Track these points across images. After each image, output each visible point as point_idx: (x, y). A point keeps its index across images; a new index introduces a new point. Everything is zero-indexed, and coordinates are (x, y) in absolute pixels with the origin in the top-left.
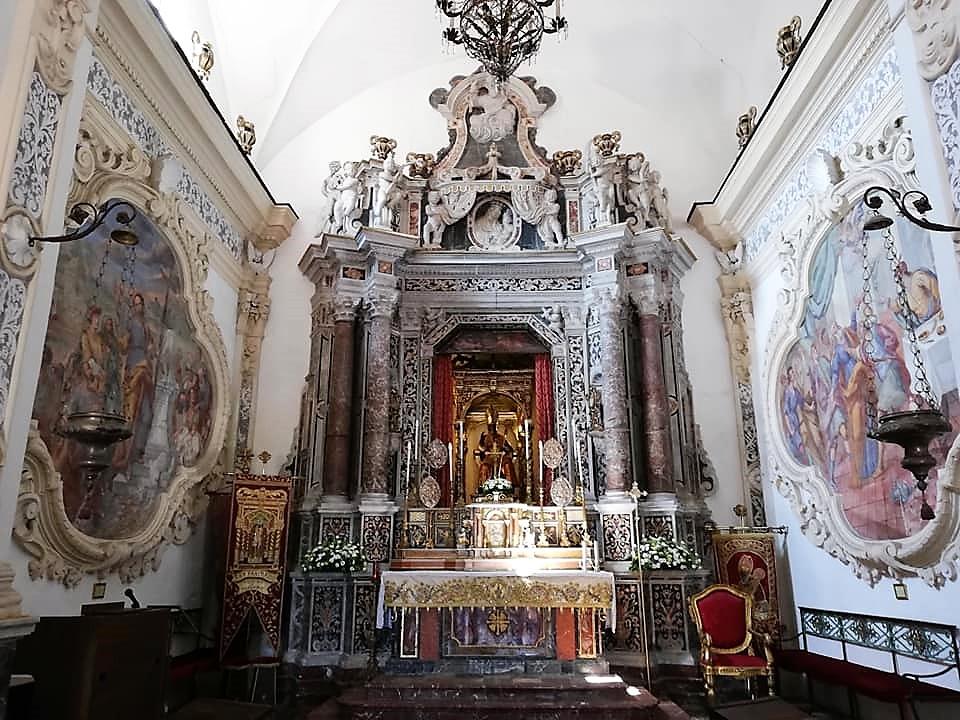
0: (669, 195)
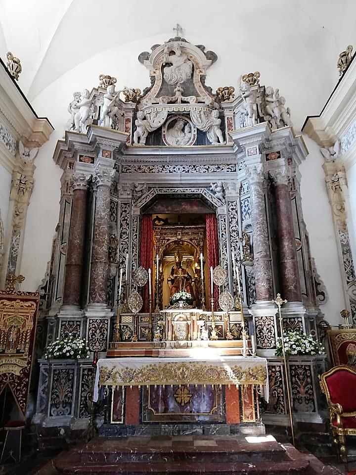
0: (291, 112)
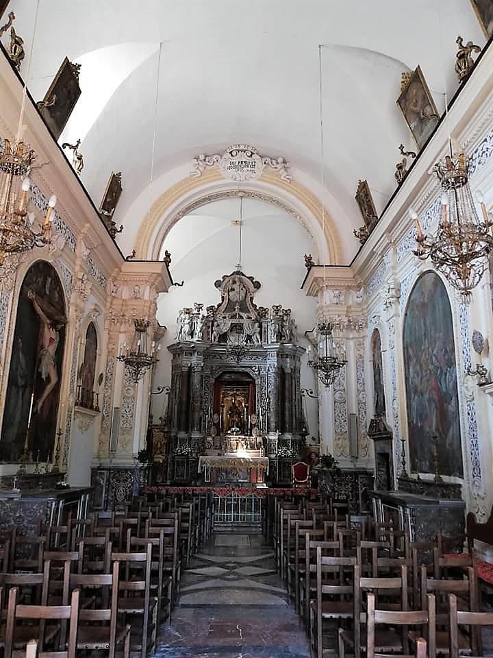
0: (298, 327)
